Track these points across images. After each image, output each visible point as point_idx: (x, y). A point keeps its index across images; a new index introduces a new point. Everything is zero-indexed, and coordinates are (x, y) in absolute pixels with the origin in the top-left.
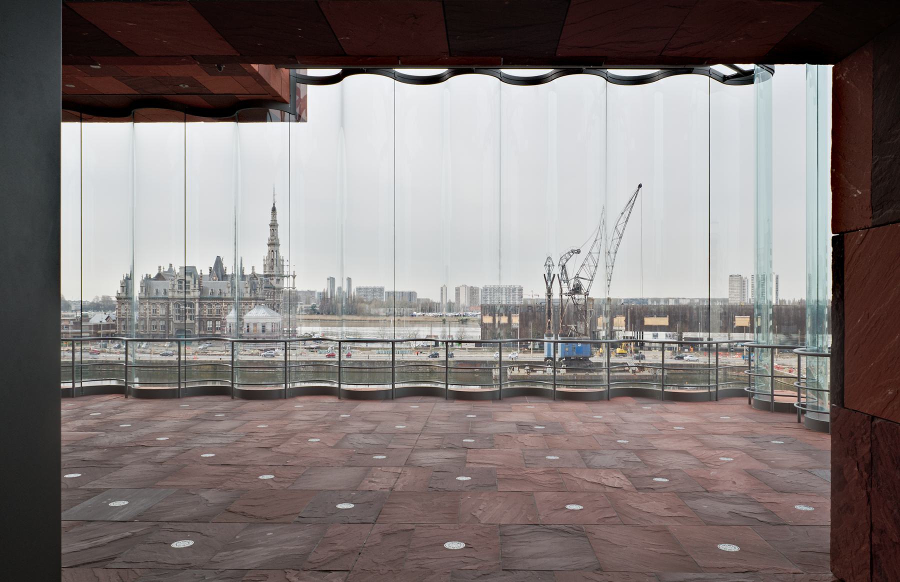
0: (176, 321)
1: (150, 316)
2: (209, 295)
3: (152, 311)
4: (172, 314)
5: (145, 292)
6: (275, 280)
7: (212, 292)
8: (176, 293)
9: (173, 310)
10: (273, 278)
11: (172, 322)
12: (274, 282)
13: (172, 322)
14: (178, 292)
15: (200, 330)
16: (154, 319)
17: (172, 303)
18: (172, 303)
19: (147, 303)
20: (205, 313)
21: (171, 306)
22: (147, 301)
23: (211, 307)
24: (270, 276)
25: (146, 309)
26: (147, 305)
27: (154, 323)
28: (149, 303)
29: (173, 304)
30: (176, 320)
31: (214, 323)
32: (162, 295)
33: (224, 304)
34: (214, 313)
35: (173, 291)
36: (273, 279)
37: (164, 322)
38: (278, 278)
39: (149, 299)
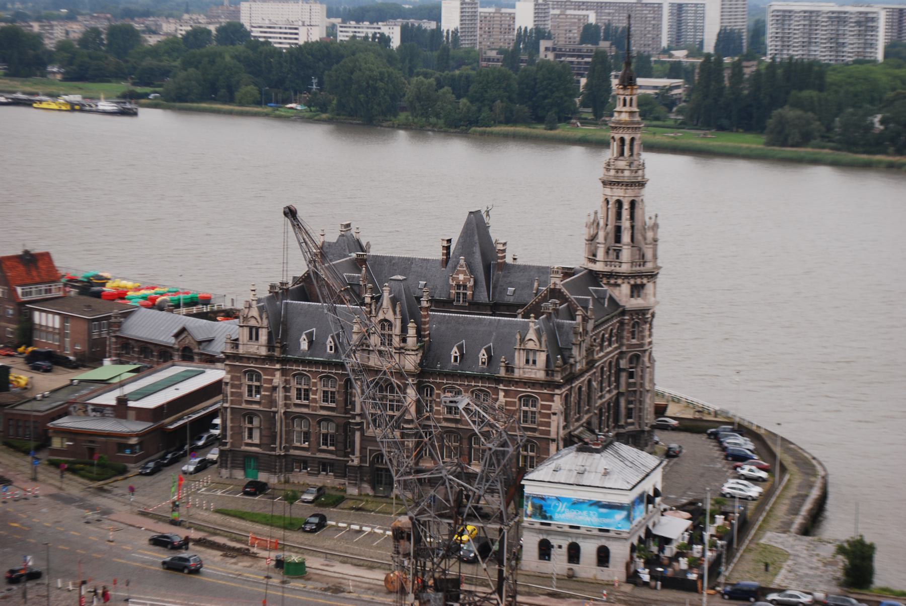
1: (286, 405)
3: (293, 393)
4: (358, 410)
6: (625, 289)
7: (462, 355)
10: (619, 281)
12: (622, 293)
13: (358, 434)
16: (301, 416)
19: (278, 374)
22: (278, 366)
24: (610, 275)
25: (275, 388)
26: (277, 379)
28: (284, 372)
33: (502, 394)
36: (617, 285)
38: (639, 281)
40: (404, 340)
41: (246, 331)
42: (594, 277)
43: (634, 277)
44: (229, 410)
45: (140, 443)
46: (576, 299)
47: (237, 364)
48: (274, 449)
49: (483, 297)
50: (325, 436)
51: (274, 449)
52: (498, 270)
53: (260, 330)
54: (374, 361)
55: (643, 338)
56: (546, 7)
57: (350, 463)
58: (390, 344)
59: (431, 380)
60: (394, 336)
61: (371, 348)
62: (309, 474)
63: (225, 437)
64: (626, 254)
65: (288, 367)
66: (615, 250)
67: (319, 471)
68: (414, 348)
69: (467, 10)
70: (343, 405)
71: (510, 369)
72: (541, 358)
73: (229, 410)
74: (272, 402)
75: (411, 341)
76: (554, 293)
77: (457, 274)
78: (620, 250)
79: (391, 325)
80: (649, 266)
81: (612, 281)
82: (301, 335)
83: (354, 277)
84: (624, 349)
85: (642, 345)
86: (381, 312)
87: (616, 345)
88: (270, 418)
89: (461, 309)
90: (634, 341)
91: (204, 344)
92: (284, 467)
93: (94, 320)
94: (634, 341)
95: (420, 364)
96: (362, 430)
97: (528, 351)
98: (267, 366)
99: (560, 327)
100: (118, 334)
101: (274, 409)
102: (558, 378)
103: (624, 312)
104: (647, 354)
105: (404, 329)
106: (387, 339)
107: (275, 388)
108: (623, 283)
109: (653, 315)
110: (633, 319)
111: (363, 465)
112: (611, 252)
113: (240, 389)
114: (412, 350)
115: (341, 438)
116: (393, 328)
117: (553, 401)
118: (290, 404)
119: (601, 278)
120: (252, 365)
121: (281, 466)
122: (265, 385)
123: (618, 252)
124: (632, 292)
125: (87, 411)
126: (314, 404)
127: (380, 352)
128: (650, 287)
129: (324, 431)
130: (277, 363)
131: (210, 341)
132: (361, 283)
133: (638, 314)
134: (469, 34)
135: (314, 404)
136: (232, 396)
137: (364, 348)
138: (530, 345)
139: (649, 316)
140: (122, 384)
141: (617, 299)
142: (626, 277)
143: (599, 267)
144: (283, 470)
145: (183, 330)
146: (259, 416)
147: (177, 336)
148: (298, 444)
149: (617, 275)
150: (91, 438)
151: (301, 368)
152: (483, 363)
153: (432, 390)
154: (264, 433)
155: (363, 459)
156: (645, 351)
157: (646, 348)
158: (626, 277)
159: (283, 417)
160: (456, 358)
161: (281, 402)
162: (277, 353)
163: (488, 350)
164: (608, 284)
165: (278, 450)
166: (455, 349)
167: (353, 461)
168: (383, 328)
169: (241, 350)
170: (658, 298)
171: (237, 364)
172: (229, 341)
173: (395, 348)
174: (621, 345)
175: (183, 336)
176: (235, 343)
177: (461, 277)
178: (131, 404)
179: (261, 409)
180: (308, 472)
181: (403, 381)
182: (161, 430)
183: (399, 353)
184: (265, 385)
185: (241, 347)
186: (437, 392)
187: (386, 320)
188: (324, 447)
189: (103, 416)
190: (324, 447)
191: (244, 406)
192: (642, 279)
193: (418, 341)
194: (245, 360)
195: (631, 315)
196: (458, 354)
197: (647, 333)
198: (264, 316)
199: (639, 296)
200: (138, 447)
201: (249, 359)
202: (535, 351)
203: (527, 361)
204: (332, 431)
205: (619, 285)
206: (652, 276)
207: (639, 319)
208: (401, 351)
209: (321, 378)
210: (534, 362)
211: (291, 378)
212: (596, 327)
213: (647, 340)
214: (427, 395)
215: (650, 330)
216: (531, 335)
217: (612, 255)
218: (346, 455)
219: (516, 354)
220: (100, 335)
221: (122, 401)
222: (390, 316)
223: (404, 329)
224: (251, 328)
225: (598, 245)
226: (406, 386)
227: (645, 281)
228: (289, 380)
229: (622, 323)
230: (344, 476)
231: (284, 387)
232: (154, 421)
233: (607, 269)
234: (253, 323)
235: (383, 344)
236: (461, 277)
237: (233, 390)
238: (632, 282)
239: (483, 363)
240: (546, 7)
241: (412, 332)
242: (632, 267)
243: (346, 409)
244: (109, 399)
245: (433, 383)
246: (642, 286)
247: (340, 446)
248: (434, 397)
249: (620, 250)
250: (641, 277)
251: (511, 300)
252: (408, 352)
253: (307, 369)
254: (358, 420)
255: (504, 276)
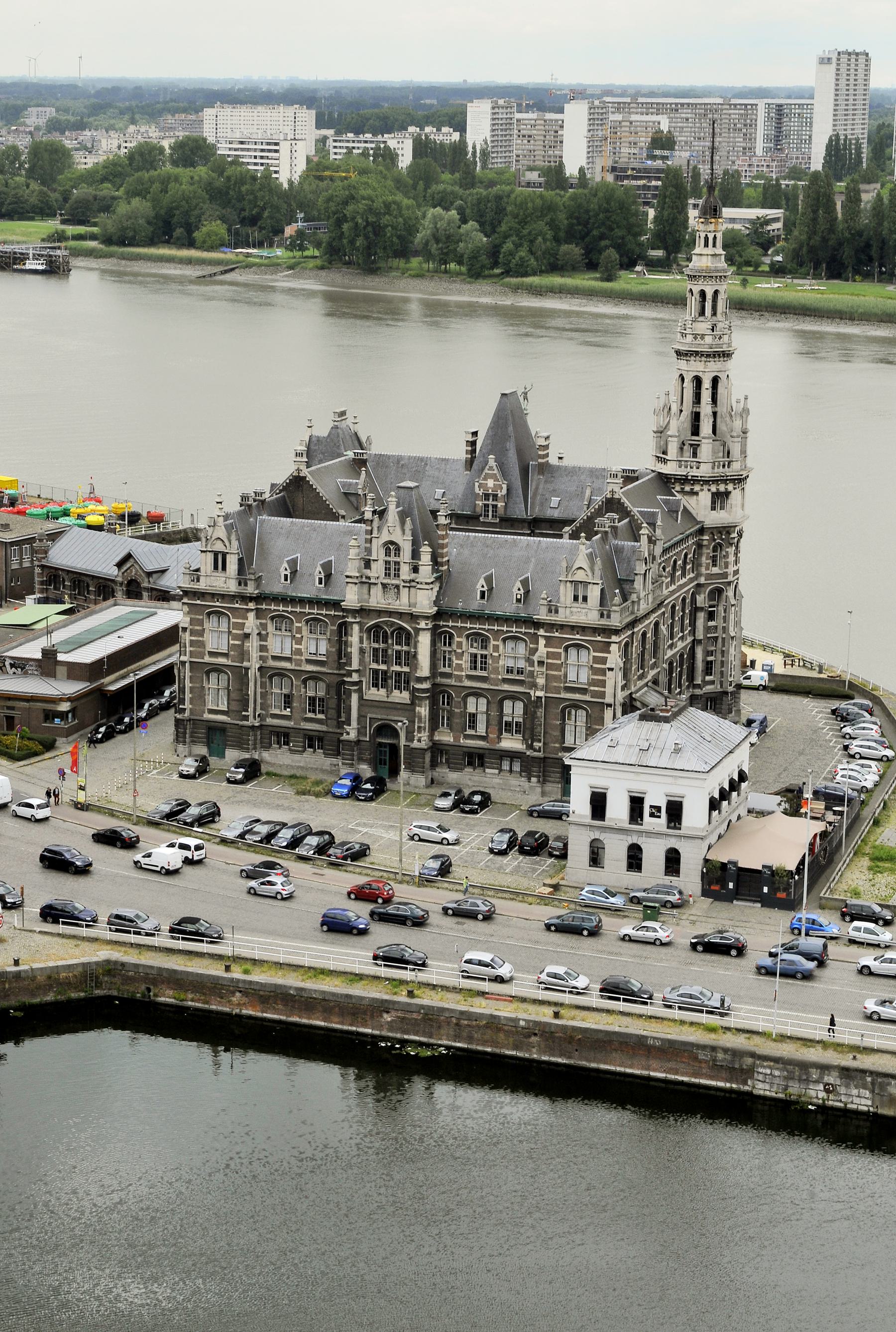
0: (373, 690)
2: (475, 604)
4: (355, 665)
5: (241, 571)
6: (705, 497)
7: (491, 589)
8: (377, 591)
9: (362, 651)
10: (697, 488)
11: (355, 698)
14: (384, 586)
15: (434, 725)
17: (356, 628)
18: (356, 628)
19: (251, 616)
20: (459, 667)
21: (355, 637)
22: (252, 605)
23: (485, 647)
25: (247, 636)
27: (277, 690)
28: (259, 614)
29: (361, 630)
30: (376, 685)
31: (494, 707)
32: (310, 588)
33: (542, 642)
34: (496, 671)
35: (366, 583)
36: (693, 493)
37: (322, 686)
38: (722, 488)
39: (259, 599)
40: (415, 570)
41: (210, 557)
42: (665, 481)
43: (716, 482)
44: (187, 665)
45: (73, 710)
46: (640, 512)
47: (198, 602)
48: (246, 718)
49: (519, 511)
50: (312, 700)
51: (246, 718)
52: (539, 474)
53: (228, 556)
54: (377, 599)
55: (726, 565)
56: (604, 110)
57: (345, 737)
58: (397, 575)
59: (450, 624)
60: (402, 564)
61: (372, 581)
62: (292, 751)
63: (182, 701)
64: (706, 450)
65: (264, 607)
66: (691, 445)
67: (304, 747)
68: (429, 581)
69: (500, 116)
70: (336, 658)
71: (553, 609)
72: (594, 593)
73: (187, 665)
74: (243, 655)
75: (426, 572)
76: (612, 504)
77: (485, 479)
78: (699, 445)
79: (398, 549)
80: (736, 466)
81: (687, 488)
82: (282, 563)
83: (350, 484)
84: (702, 580)
85: (725, 575)
86: (385, 531)
87: (692, 575)
88: (241, 675)
89: (489, 528)
90: (715, 570)
91: (155, 576)
92: (258, 741)
93: (12, 544)
94: (715, 570)
95: (436, 603)
96: (360, 691)
97: (575, 583)
98: (237, 606)
99: (619, 550)
100: (44, 562)
101: (245, 664)
102: (616, 621)
103: (702, 531)
104: (733, 587)
105: (416, 554)
106: (391, 569)
107: (247, 636)
108: (702, 490)
109: (740, 535)
110: (715, 540)
111: (361, 739)
112: (685, 447)
113: (202, 636)
114: (426, 583)
115: (333, 703)
116: (401, 554)
117: (609, 652)
118: (267, 657)
119: (673, 484)
120: (218, 604)
121: (255, 740)
122: (234, 631)
123: (695, 448)
124: (713, 502)
125: (4, 666)
126: (298, 657)
127: (384, 586)
128: (736, 495)
129: (311, 693)
130: (251, 601)
131: (163, 571)
132: (360, 492)
133: (720, 533)
134: (503, 149)
135: (298, 657)
136: (191, 646)
137: (364, 580)
138: (580, 576)
139: (735, 535)
140: (49, 631)
141: (693, 512)
142: (707, 482)
143: (669, 469)
144: (258, 746)
145: (129, 556)
146: (227, 673)
147: (120, 565)
148: (277, 712)
149: (695, 481)
150: (10, 703)
151: (281, 608)
152: (518, 601)
153: (451, 636)
154: (233, 695)
155: (361, 731)
156: (729, 583)
157: (730, 578)
158: (707, 482)
159: (258, 674)
160: (483, 593)
161: (255, 654)
162: (251, 589)
163: (525, 583)
164: (682, 492)
165: (251, 718)
166: (482, 582)
167: (348, 734)
168: (388, 553)
169: (202, 585)
170: (747, 511)
171: (198, 602)
172: (187, 571)
173: (403, 581)
174: (699, 575)
175: (128, 565)
176: (195, 574)
177: (490, 483)
178: (61, 657)
179: (230, 663)
180: (290, 750)
181: (413, 625)
182: (100, 692)
183: (409, 587)
184: (234, 631)
185: (202, 579)
186: (459, 639)
187: (392, 543)
188: (310, 715)
189: (26, 674)
190: (310, 715)
191: (207, 659)
192: (727, 484)
193: (434, 571)
194: (208, 597)
195: (712, 533)
196: (485, 588)
197: (732, 558)
198: (233, 537)
199: (722, 508)
200: (70, 715)
201: (213, 596)
202: (586, 584)
203: (576, 598)
204: (321, 693)
205: (697, 494)
206: (739, 481)
207: (722, 540)
208: (411, 584)
209: (307, 621)
210: (585, 599)
211: (269, 622)
212: (665, 551)
213: (731, 569)
214: (445, 644)
215: (736, 554)
216: (582, 561)
217: (687, 455)
218: (340, 725)
219: (562, 588)
220: (21, 563)
221: (49, 654)
222: (397, 537)
223: (416, 554)
224: (216, 554)
225: (670, 439)
226: (417, 631)
227: (730, 487)
228: (266, 624)
229: (700, 546)
230: (337, 754)
231: (259, 634)
232: (91, 680)
233: (682, 472)
234: (219, 547)
235: (387, 575)
236: (490, 483)
237: (193, 638)
238: (714, 488)
239: (518, 601)
240: (604, 110)
241: (426, 557)
242: (713, 468)
243: (339, 663)
244: (32, 650)
245: (453, 627)
246: (727, 494)
247: (332, 713)
248: (454, 646)
249: (699, 445)
250: (725, 482)
251: (556, 514)
252: (419, 586)
253: (290, 609)
254: (355, 677)
255: (546, 482)
